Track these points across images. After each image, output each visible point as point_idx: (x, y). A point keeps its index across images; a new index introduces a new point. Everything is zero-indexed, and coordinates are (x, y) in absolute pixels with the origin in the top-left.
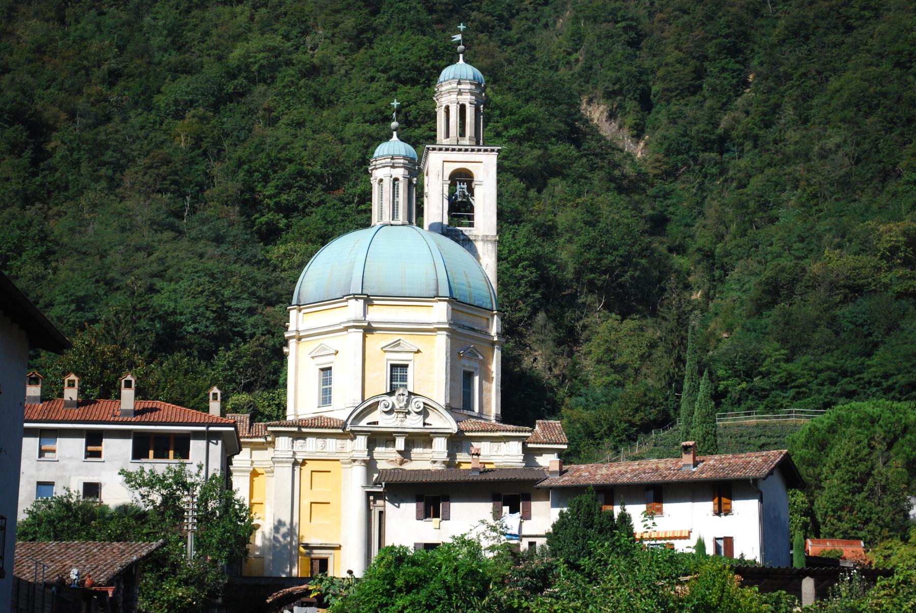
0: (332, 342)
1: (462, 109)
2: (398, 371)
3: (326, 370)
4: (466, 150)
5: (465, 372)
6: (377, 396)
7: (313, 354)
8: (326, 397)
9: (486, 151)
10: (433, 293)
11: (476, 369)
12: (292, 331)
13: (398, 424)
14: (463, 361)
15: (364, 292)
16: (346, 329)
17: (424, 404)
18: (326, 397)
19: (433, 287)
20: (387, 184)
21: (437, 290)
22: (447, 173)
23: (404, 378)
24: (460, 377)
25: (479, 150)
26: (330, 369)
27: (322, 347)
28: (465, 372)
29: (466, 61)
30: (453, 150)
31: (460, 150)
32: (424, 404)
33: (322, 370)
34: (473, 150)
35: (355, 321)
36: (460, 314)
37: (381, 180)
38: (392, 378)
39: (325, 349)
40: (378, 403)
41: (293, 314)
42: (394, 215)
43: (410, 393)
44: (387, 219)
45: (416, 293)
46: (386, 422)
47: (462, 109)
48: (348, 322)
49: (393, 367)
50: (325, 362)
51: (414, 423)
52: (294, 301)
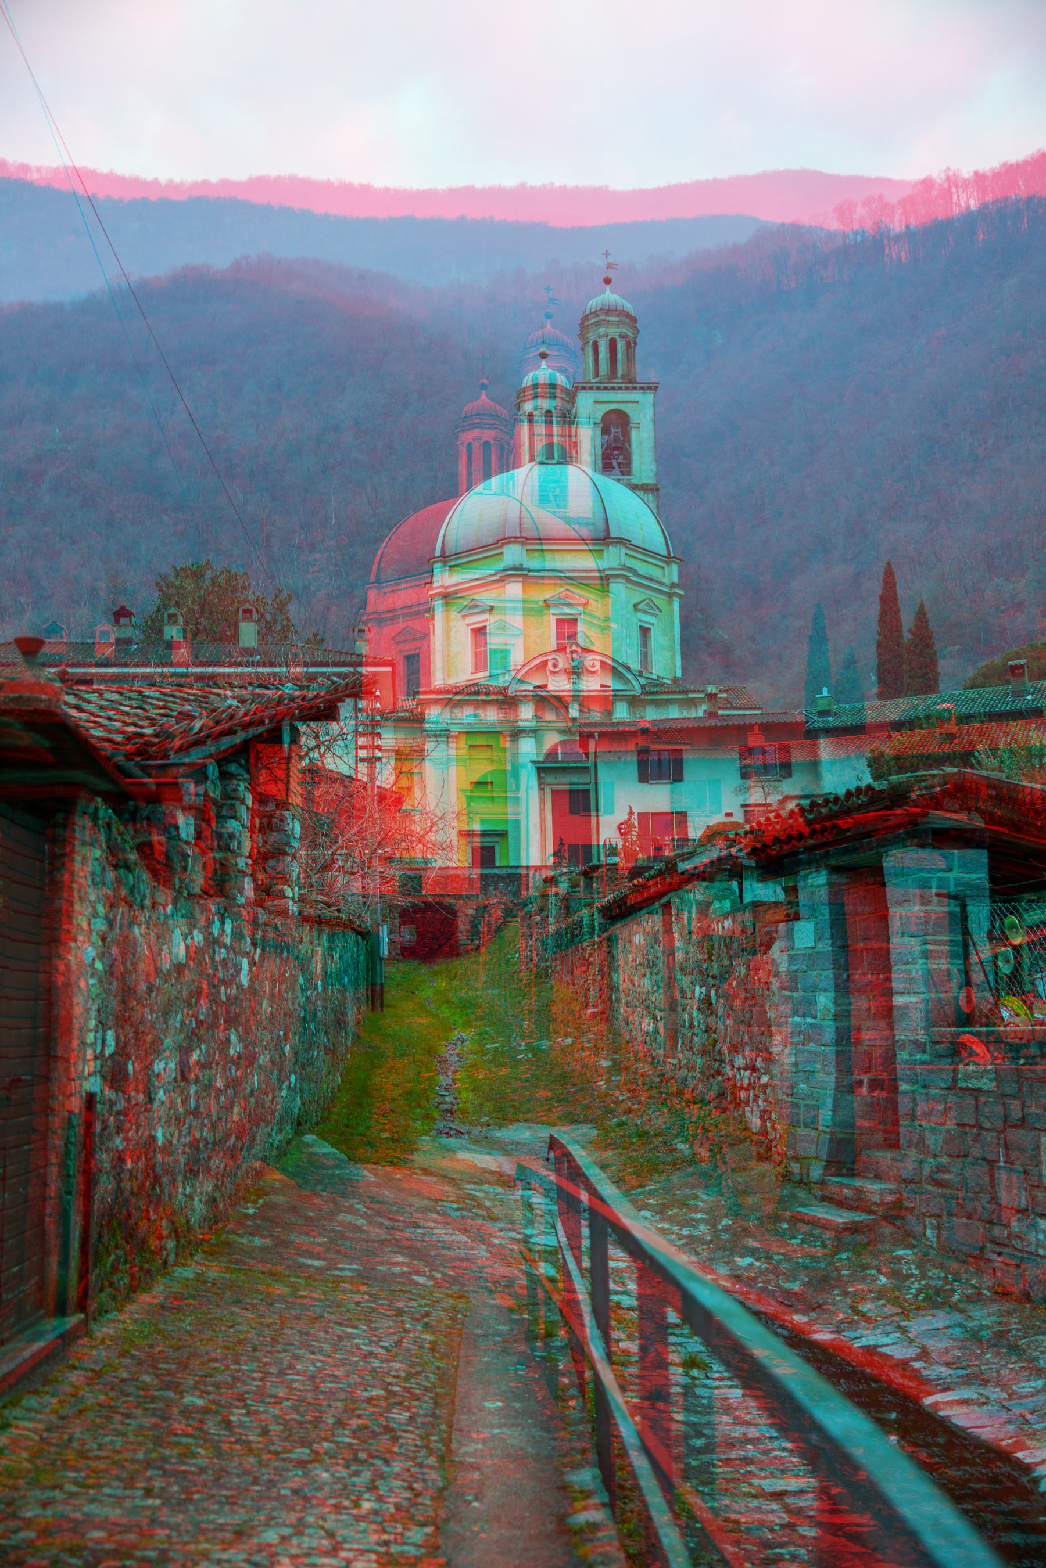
0: (486, 597)
1: (613, 344)
2: (567, 627)
3: (479, 632)
4: (620, 388)
5: (641, 627)
6: (545, 654)
8: (480, 662)
9: (642, 388)
10: (602, 535)
13: (569, 687)
14: (641, 616)
15: (524, 534)
16: (502, 580)
20: (539, 417)
21: (607, 530)
22: (599, 415)
23: (573, 636)
24: (636, 634)
25: (635, 388)
28: (641, 627)
29: (612, 292)
30: (605, 388)
31: (613, 388)
34: (627, 388)
37: (531, 416)
38: (559, 636)
39: (476, 606)
40: (546, 663)
41: (437, 568)
43: (583, 649)
47: (613, 344)
48: (505, 570)
49: (559, 622)
50: (477, 620)
51: (591, 684)
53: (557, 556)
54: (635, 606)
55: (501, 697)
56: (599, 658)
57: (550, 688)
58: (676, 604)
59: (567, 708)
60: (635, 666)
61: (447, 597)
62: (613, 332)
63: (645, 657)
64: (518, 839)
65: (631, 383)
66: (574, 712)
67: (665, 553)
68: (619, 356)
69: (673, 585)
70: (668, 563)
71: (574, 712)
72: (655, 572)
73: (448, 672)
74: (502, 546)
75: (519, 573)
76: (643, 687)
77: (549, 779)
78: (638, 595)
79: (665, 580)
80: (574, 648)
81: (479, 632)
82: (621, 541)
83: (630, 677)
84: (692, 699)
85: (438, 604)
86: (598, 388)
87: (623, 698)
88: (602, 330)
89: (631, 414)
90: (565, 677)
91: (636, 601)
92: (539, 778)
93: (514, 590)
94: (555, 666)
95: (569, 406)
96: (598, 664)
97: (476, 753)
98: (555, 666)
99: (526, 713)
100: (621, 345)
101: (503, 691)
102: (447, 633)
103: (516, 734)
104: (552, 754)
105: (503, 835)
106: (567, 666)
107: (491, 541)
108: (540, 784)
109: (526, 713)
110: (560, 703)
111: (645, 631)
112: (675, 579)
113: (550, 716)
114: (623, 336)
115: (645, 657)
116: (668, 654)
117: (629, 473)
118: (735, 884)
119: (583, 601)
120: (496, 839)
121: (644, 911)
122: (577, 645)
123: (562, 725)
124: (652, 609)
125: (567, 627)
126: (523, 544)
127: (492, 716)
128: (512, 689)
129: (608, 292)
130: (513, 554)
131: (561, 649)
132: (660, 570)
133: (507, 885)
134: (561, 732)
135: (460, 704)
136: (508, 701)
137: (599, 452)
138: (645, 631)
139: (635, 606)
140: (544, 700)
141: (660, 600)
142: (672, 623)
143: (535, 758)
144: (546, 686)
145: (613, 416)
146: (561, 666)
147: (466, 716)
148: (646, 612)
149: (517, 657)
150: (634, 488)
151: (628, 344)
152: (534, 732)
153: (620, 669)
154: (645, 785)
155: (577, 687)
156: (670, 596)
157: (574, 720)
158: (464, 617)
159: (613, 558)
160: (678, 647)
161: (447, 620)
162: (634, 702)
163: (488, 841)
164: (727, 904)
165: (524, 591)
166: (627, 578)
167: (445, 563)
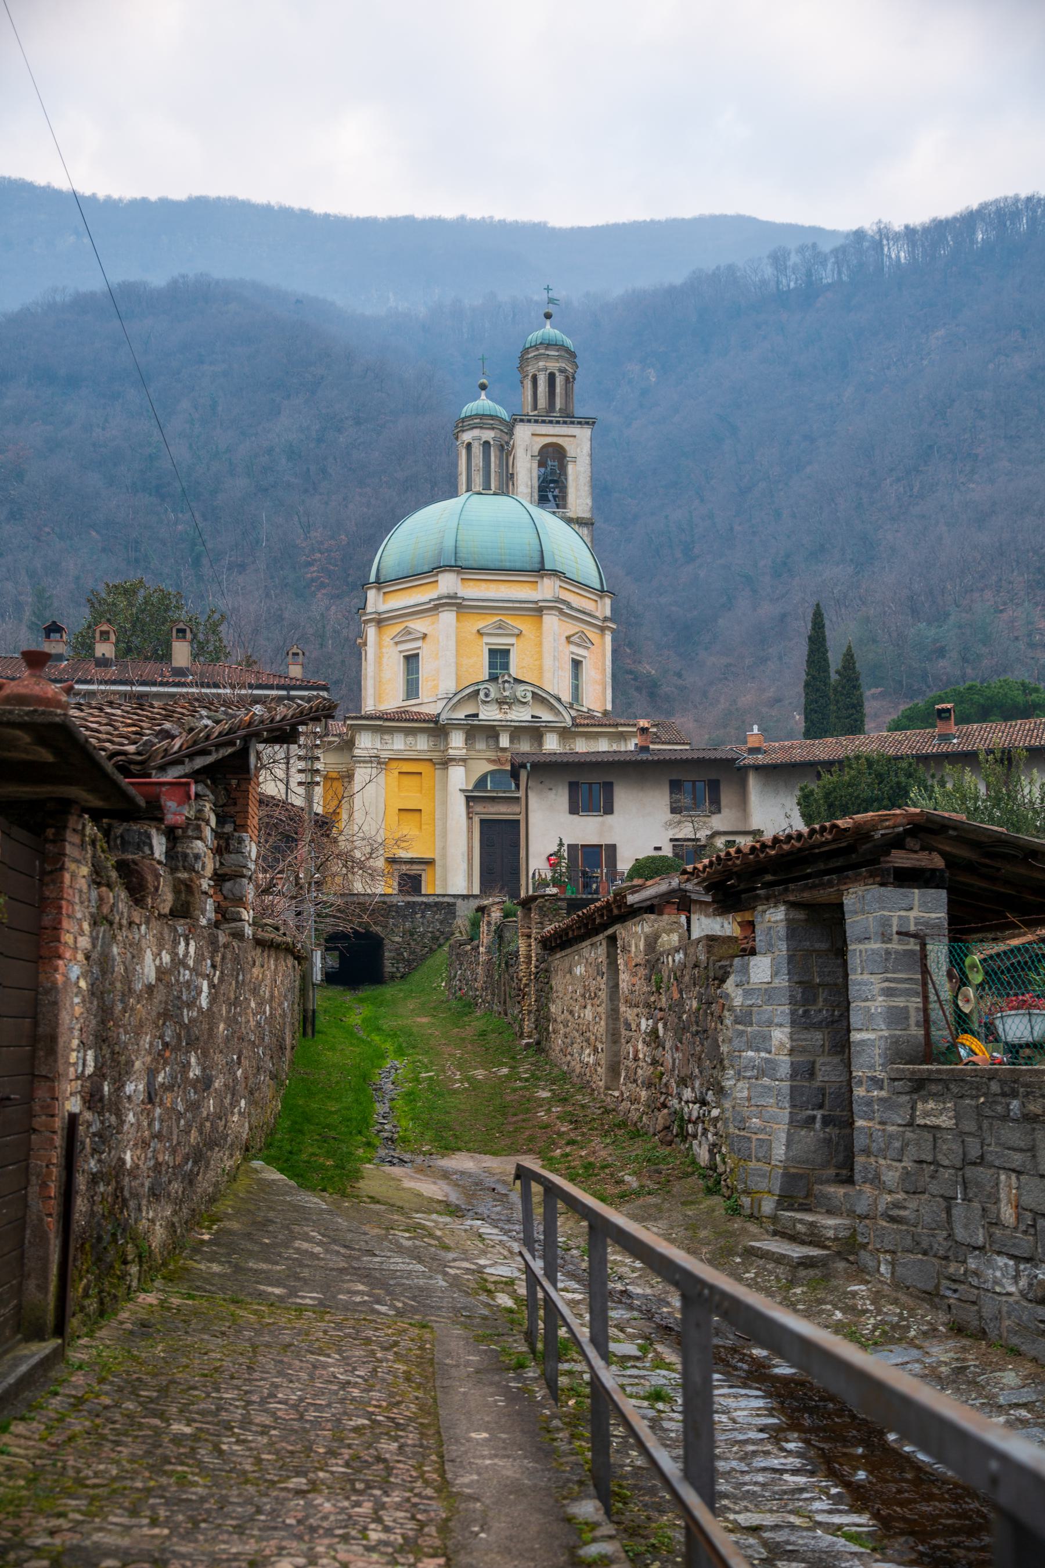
0: (419, 625)
1: (552, 378)
2: (499, 658)
3: (411, 660)
4: (558, 422)
5: (573, 660)
6: (477, 683)
7: (396, 640)
8: (412, 689)
9: (580, 423)
10: (537, 566)
11: (585, 657)
12: (371, 613)
14: (574, 648)
15: (459, 564)
16: (436, 607)
17: (533, 692)
18: (412, 689)
19: (537, 559)
20: (477, 450)
23: (506, 666)
24: (568, 666)
25: (572, 423)
26: (417, 655)
27: (407, 631)
28: (573, 660)
29: (552, 327)
30: (543, 422)
31: (551, 422)
32: (533, 692)
33: (407, 658)
34: (565, 423)
35: (449, 597)
36: (567, 592)
37: (469, 446)
38: (492, 665)
39: (410, 633)
41: (371, 594)
42: (487, 486)
43: (515, 679)
44: (478, 486)
45: (518, 566)
46: (489, 714)
47: (552, 378)
48: (439, 599)
51: (521, 715)
52: (372, 578)
53: (493, 586)
54: (568, 638)
55: (432, 725)
56: (530, 688)
57: (481, 717)
58: (608, 638)
59: (496, 738)
60: (566, 697)
61: (380, 622)
62: (553, 366)
63: (576, 689)
64: (444, 867)
65: (568, 418)
66: (504, 741)
67: (598, 587)
68: (558, 390)
69: (605, 619)
70: (601, 597)
71: (504, 741)
72: (588, 605)
73: (378, 698)
74: (437, 575)
75: (454, 603)
76: (573, 719)
77: (478, 808)
78: (572, 628)
79: (598, 614)
80: (506, 678)
81: (411, 660)
82: (556, 573)
83: (561, 709)
84: (622, 733)
85: (371, 631)
86: (536, 421)
87: (553, 729)
88: (541, 364)
89: (567, 448)
90: (496, 707)
91: (567, 634)
92: (468, 806)
93: (448, 617)
94: (487, 695)
95: (506, 438)
96: (530, 695)
97: (407, 781)
98: (487, 695)
99: (457, 741)
100: (559, 380)
101: (435, 719)
102: (379, 658)
103: (446, 763)
104: (481, 783)
105: (430, 863)
106: (498, 696)
107: (426, 569)
108: (468, 813)
109: (457, 741)
110: (491, 732)
111: (577, 664)
112: (608, 613)
113: (481, 745)
114: (562, 371)
115: (576, 689)
116: (599, 688)
117: (565, 507)
118: (683, 919)
119: (516, 632)
120: (422, 867)
121: (588, 942)
122: (510, 675)
123: (492, 755)
124: (584, 642)
125: (499, 658)
126: (458, 573)
127: (422, 744)
128: (443, 717)
129: (548, 327)
130: (448, 583)
131: (493, 678)
132: (593, 603)
133: (435, 913)
134: (490, 761)
135: (391, 730)
136: (437, 729)
137: (536, 485)
138: (577, 664)
139: (568, 638)
140: (475, 730)
141: (592, 634)
142: (604, 655)
143: (464, 788)
144: (477, 715)
145: (550, 449)
146: (492, 695)
147: (398, 743)
148: (578, 645)
149: (448, 685)
150: (569, 521)
151: (567, 379)
152: (464, 760)
153: (552, 700)
154: (575, 816)
155: (509, 717)
156: (602, 629)
157: (504, 750)
158: (397, 643)
159: (547, 589)
160: (609, 680)
161: (379, 645)
162: (565, 733)
163: (415, 869)
164: (675, 938)
165: (458, 620)
166: (560, 610)
167: (379, 589)
